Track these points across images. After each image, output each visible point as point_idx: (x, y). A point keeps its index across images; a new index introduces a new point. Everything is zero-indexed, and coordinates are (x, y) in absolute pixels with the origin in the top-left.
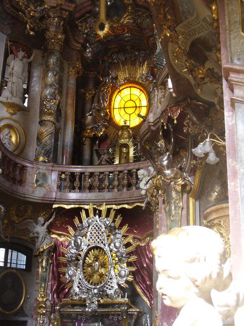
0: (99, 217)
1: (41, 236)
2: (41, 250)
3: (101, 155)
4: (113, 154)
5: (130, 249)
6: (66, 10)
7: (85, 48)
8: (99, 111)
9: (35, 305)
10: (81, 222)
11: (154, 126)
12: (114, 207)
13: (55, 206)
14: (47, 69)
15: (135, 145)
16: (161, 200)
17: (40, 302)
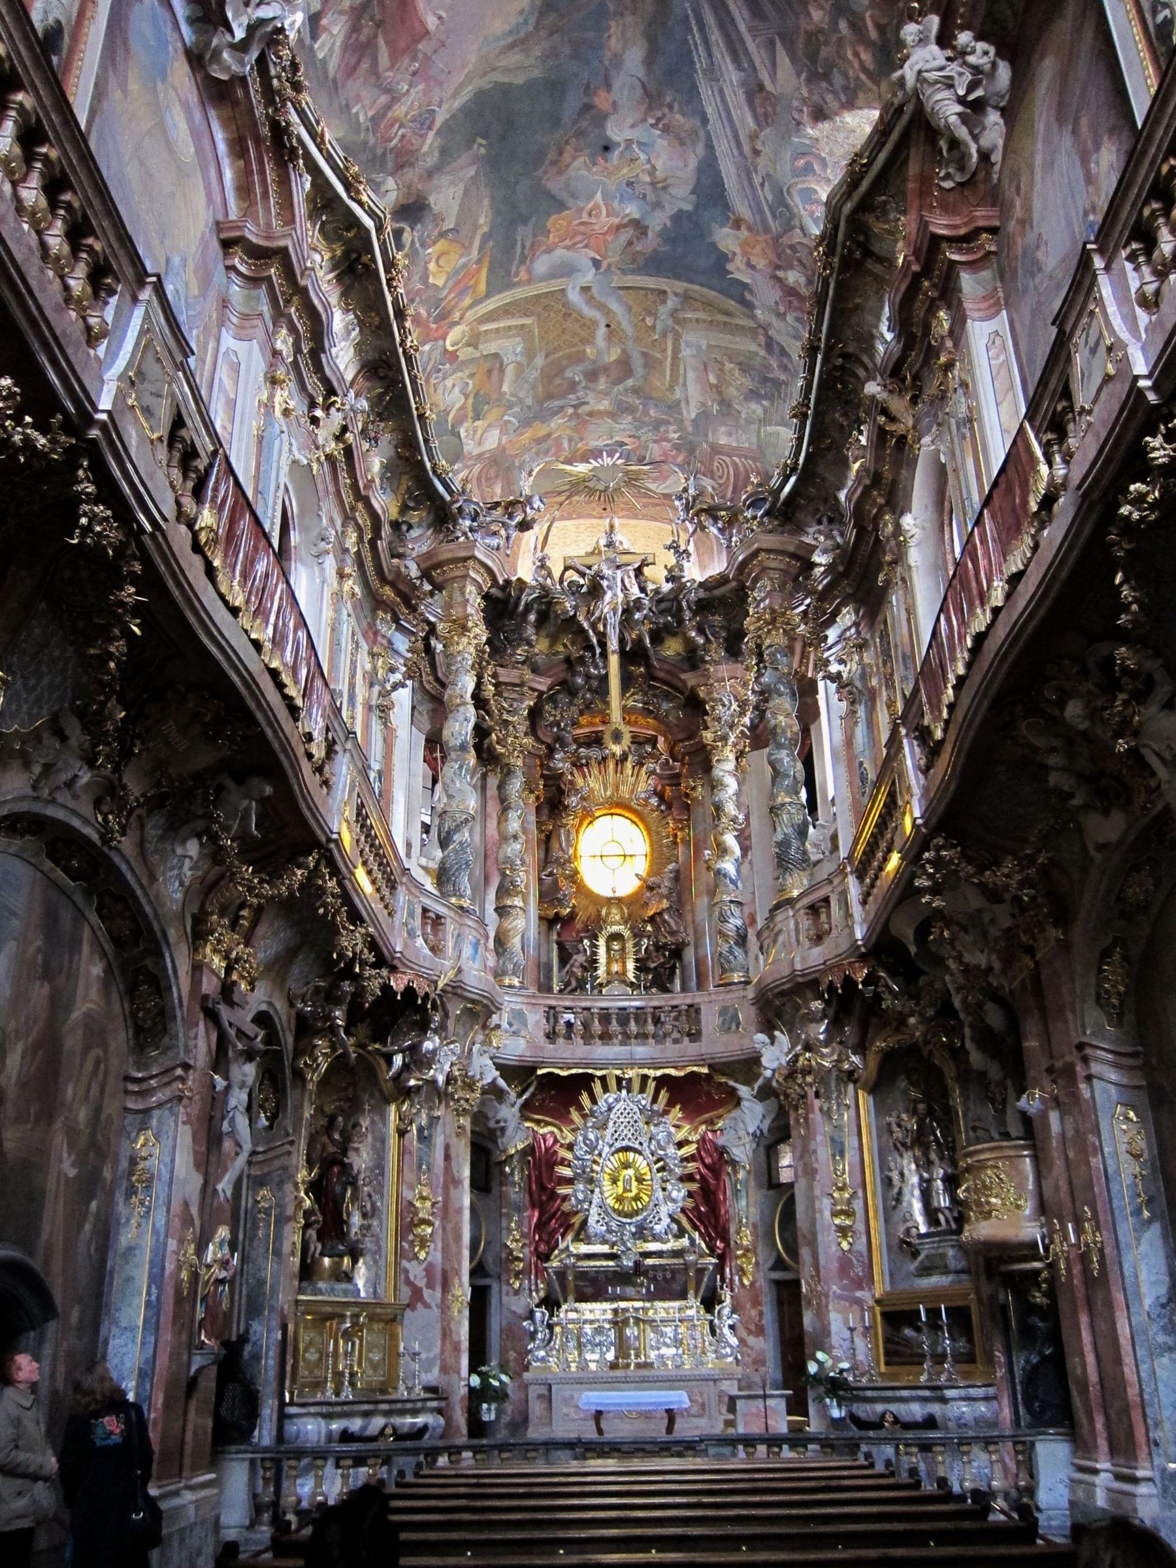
0: (629, 1092)
1: (511, 1125)
2: (513, 1151)
3: (571, 956)
4: (594, 954)
5: (691, 1149)
6: (533, 689)
7: (551, 750)
8: (562, 865)
9: (504, 1256)
10: (594, 1101)
11: (803, 976)
12: (652, 1073)
13: (540, 1072)
14: (505, 806)
15: (635, 936)
16: (811, 1092)
17: (511, 1252)
